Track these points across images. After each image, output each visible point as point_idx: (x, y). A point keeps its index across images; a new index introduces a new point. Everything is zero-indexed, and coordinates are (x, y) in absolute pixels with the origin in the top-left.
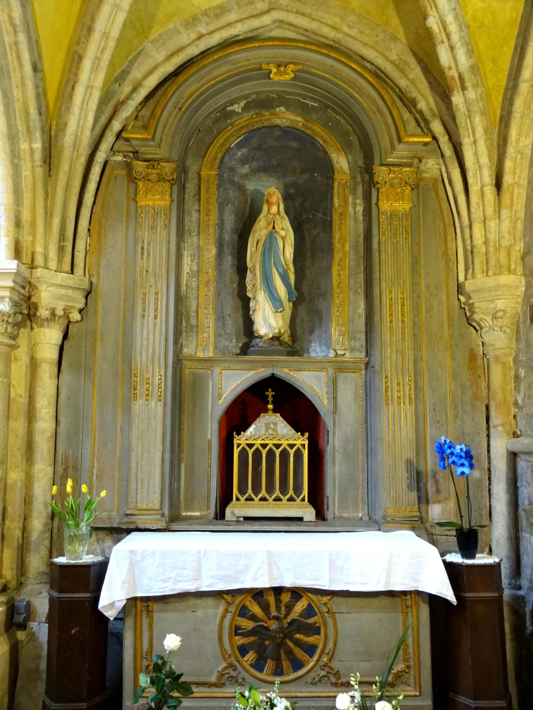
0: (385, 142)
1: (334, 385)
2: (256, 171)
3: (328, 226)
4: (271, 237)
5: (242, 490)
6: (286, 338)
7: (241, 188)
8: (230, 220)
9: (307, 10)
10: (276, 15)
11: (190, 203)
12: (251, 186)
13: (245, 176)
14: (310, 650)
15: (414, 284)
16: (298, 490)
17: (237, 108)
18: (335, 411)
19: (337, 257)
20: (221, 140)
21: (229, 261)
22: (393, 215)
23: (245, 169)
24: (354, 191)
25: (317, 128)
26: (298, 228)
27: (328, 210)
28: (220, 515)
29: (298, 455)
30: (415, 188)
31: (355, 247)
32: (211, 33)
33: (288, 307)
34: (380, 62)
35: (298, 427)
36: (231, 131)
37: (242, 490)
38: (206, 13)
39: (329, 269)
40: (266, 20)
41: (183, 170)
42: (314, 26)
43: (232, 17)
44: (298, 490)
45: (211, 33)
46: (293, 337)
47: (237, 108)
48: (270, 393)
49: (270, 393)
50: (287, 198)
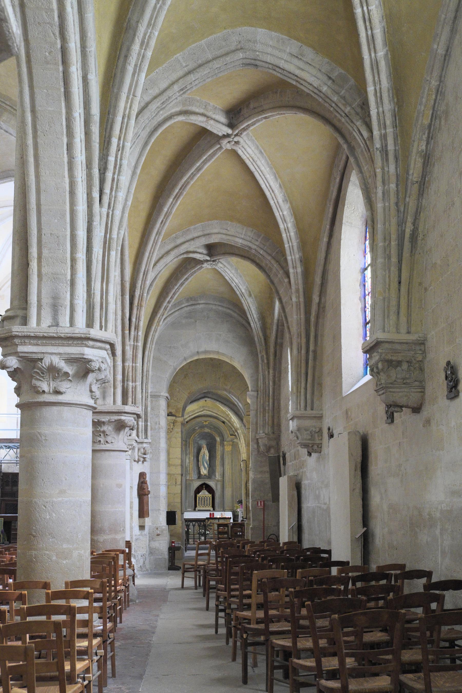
0: (226, 437)
1: (216, 485)
2: (200, 439)
3: (215, 452)
4: (204, 455)
5: (199, 505)
6: (207, 475)
7: (198, 443)
8: (195, 451)
9: (211, 410)
10: (205, 411)
11: (188, 449)
12: (200, 442)
13: (199, 441)
14: (211, 529)
15: (232, 465)
16: (210, 505)
17: (197, 428)
18: (217, 490)
19: (217, 459)
20: (194, 435)
21: (195, 459)
22: (228, 451)
23: (199, 439)
24: (221, 446)
25: (213, 432)
26: (210, 452)
27: (215, 449)
28: (195, 510)
29: (210, 498)
30: (232, 445)
31: (221, 457)
32: (192, 415)
33: (207, 469)
34: (225, 421)
35: (209, 492)
36: (195, 433)
37: (199, 505)
38: (191, 411)
39: (215, 461)
40: (202, 412)
41: (186, 441)
42: (212, 413)
43: (196, 412)
44: (210, 505)
45: (192, 415)
46: (209, 474)
47: (197, 428)
48: (204, 486)
49: (204, 486)
50: (207, 445)
